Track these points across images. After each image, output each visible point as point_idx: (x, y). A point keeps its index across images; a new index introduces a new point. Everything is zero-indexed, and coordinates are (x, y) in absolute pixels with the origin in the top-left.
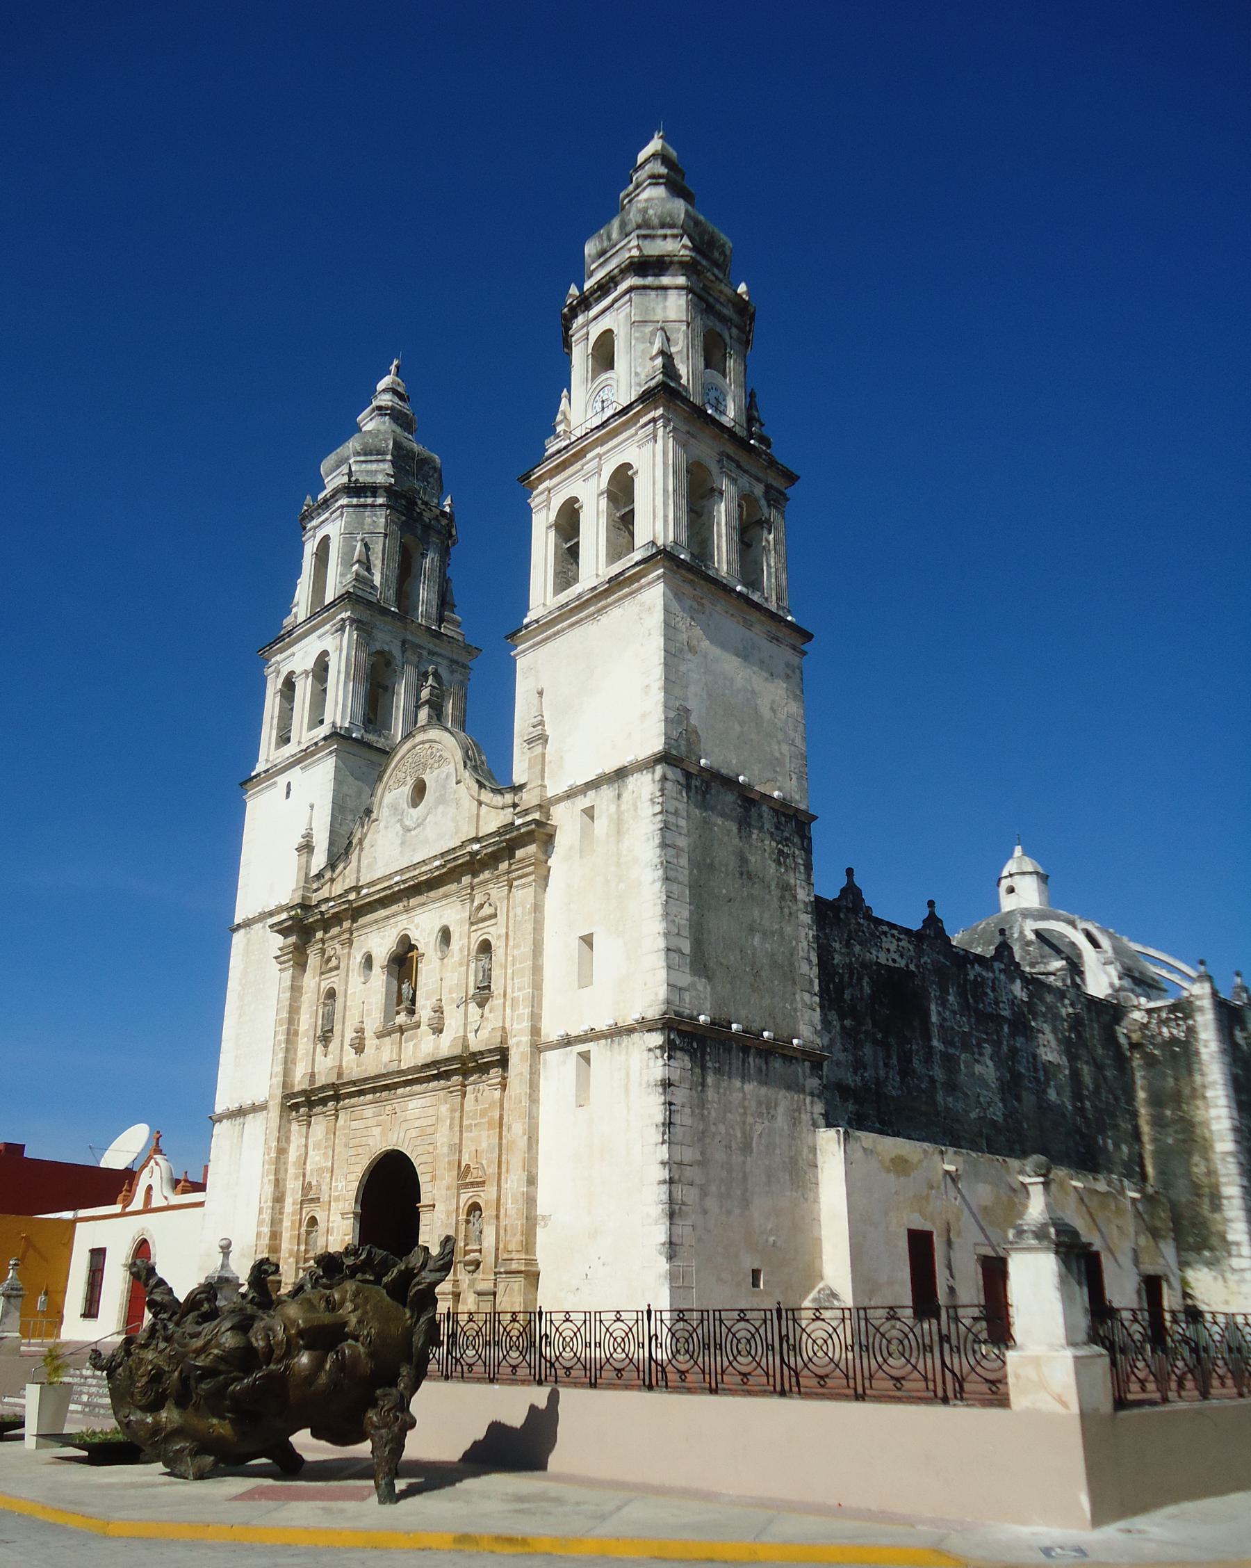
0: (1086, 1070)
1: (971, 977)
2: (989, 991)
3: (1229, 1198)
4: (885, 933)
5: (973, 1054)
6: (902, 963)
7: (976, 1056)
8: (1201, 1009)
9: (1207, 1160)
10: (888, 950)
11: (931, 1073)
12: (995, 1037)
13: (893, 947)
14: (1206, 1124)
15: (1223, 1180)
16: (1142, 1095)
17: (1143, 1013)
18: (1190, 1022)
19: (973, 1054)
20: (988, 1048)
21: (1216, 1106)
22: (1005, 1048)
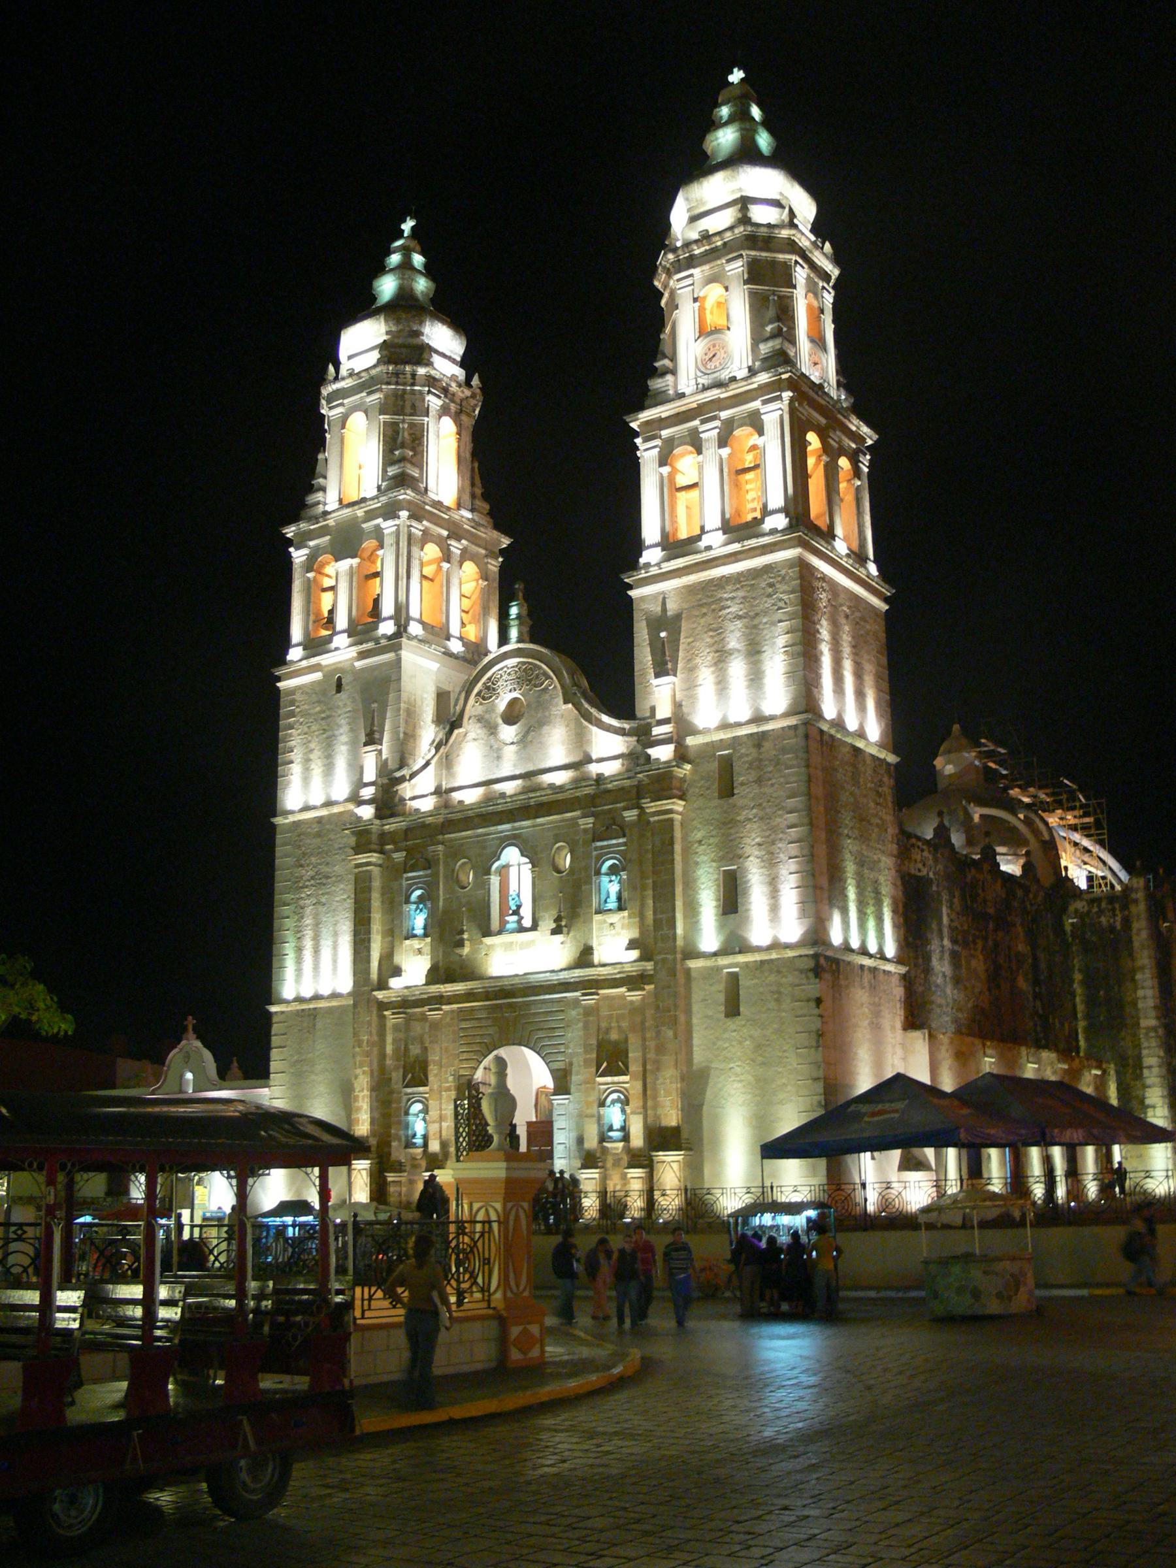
0: (1042, 956)
1: (969, 877)
2: (980, 891)
3: (1150, 1067)
4: (913, 845)
5: (970, 949)
6: (924, 872)
7: (972, 952)
8: (1136, 901)
9: (1135, 1035)
10: (916, 861)
11: (943, 970)
12: (984, 933)
13: (919, 858)
14: (1134, 1004)
15: (1145, 1052)
16: (1078, 976)
17: (1085, 903)
18: (1126, 913)
19: (970, 949)
20: (980, 943)
21: (1143, 988)
22: (990, 943)
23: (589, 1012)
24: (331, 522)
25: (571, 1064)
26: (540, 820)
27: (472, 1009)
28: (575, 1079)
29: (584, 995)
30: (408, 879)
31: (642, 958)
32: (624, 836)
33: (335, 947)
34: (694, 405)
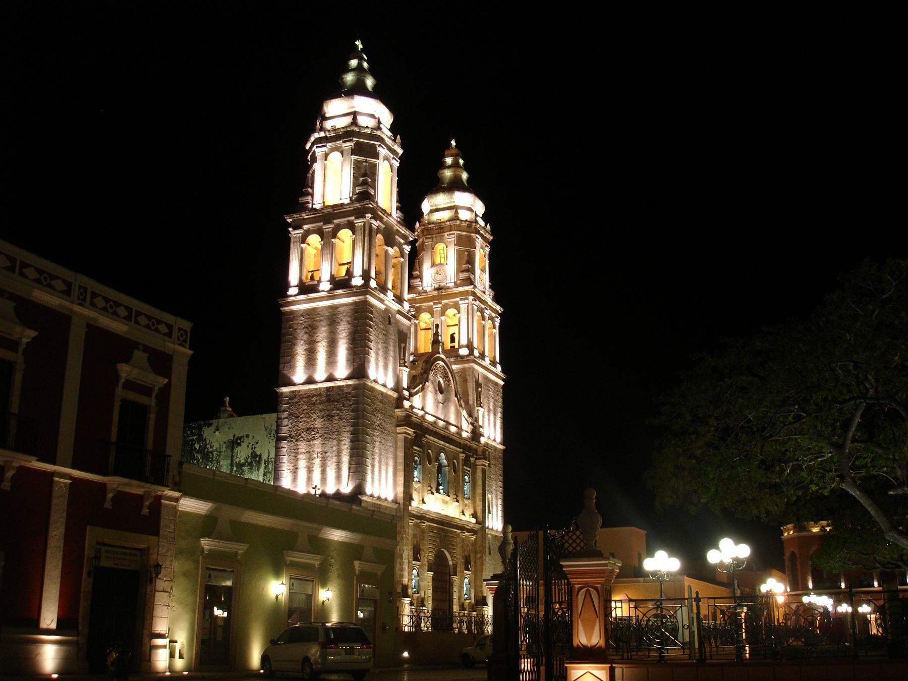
23: (463, 540)
24: (385, 219)
25: (457, 562)
26: (451, 446)
27: (433, 527)
28: (458, 569)
29: (461, 533)
30: (416, 450)
31: (477, 522)
32: (470, 468)
33: (387, 472)
34: (484, 299)
